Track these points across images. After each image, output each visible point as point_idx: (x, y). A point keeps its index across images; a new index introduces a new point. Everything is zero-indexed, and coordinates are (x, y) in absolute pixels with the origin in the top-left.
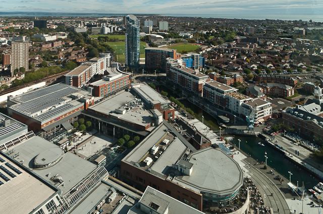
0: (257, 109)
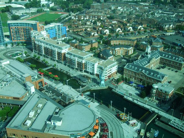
0: (107, 69)
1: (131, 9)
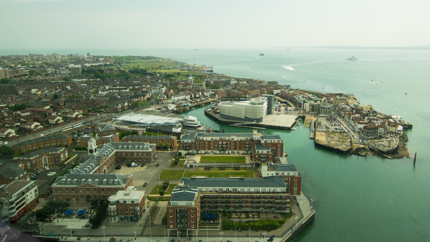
1: (57, 89)
